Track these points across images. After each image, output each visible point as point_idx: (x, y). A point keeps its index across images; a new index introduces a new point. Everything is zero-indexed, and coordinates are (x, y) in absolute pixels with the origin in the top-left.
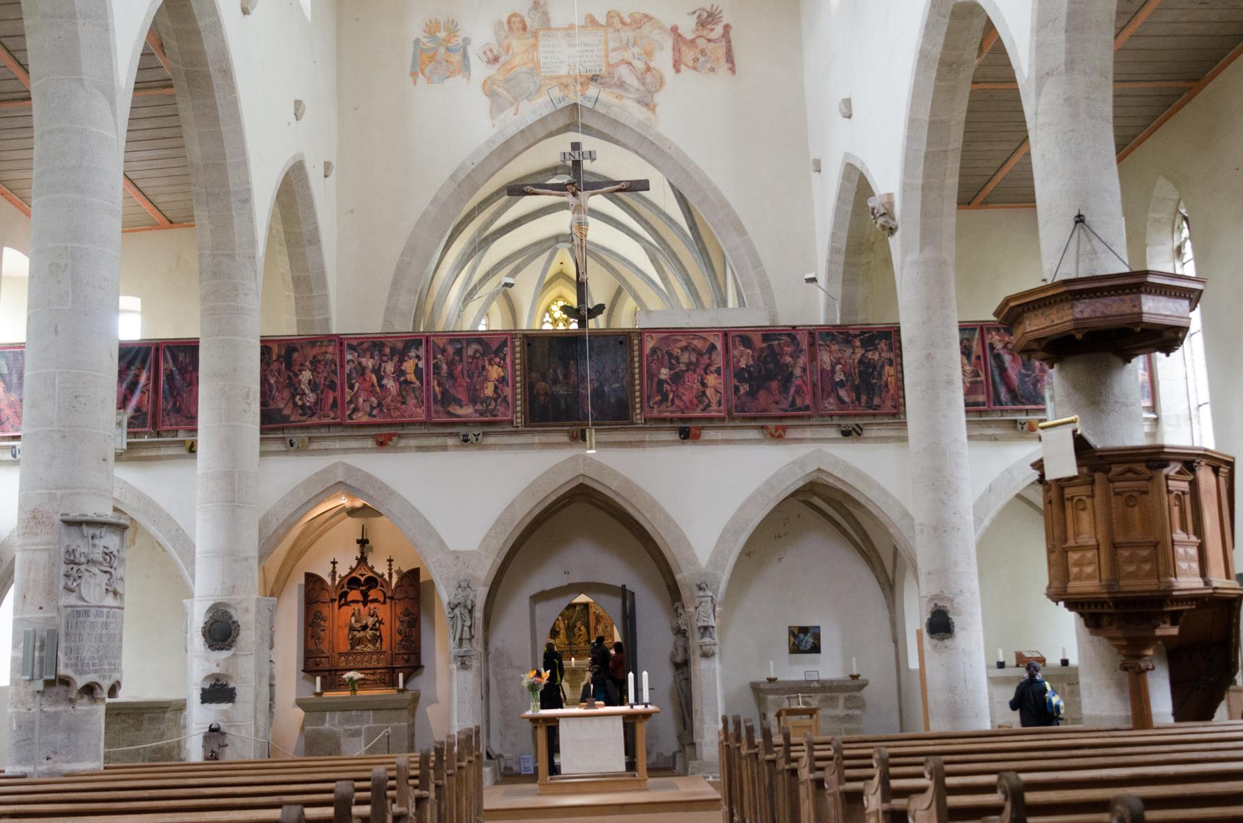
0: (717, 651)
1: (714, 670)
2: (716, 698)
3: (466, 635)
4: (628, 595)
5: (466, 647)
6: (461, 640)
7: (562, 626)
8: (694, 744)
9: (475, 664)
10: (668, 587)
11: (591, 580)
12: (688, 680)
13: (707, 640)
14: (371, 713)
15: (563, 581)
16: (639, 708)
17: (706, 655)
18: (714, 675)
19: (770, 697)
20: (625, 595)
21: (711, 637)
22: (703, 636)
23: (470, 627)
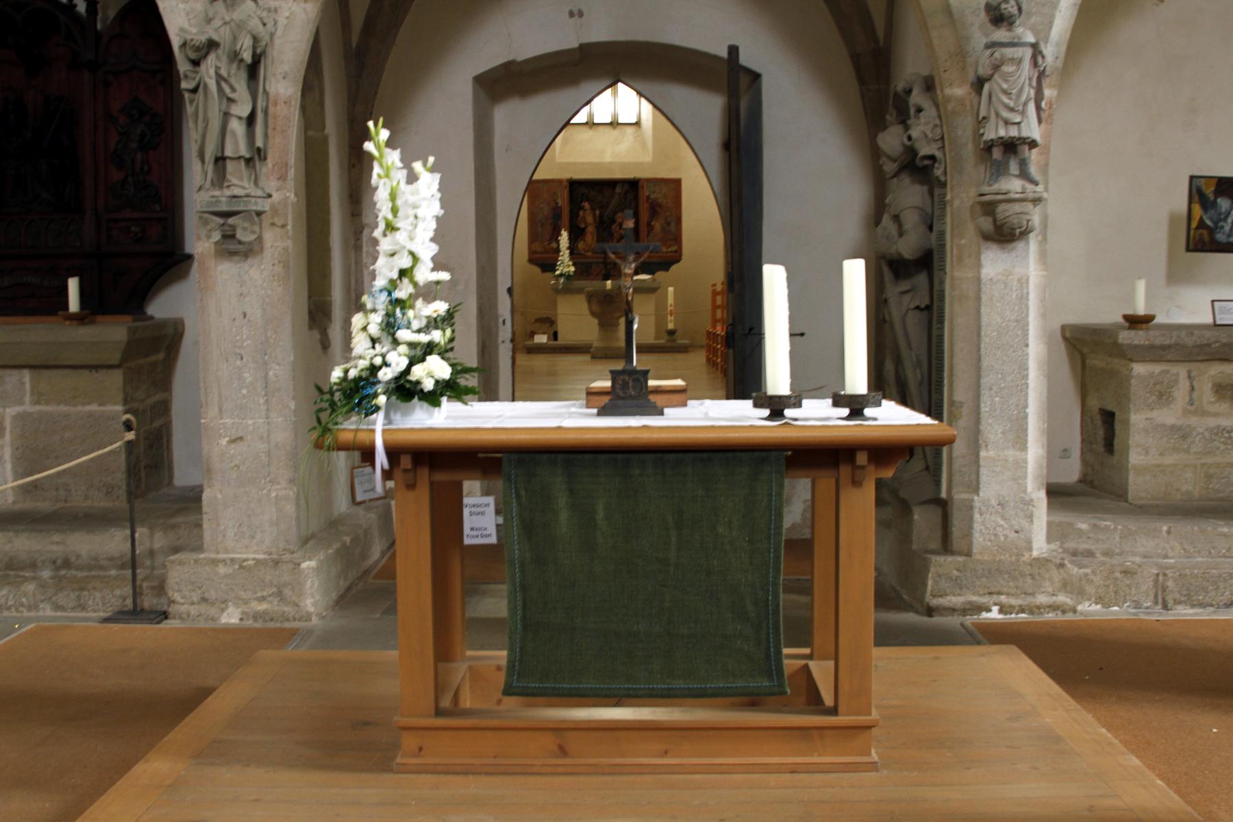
0: (1036, 220)
1: (1023, 282)
2: (1024, 368)
3: (237, 144)
4: (744, 80)
5: (239, 182)
6: (220, 160)
7: (590, 219)
8: (943, 505)
9: (280, 243)
10: (855, 58)
11: (640, 37)
12: (932, 312)
13: (1014, 185)
14: (26, 375)
15: (563, 38)
16: (817, 415)
17: (1005, 234)
18: (1023, 298)
19: (1139, 369)
20: (734, 82)
21: (1024, 175)
22: (999, 170)
23: (251, 120)
